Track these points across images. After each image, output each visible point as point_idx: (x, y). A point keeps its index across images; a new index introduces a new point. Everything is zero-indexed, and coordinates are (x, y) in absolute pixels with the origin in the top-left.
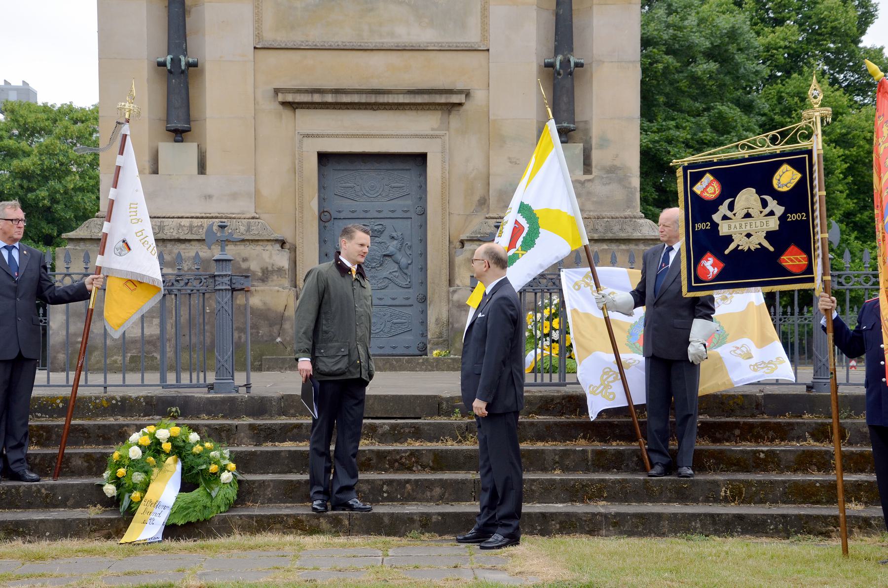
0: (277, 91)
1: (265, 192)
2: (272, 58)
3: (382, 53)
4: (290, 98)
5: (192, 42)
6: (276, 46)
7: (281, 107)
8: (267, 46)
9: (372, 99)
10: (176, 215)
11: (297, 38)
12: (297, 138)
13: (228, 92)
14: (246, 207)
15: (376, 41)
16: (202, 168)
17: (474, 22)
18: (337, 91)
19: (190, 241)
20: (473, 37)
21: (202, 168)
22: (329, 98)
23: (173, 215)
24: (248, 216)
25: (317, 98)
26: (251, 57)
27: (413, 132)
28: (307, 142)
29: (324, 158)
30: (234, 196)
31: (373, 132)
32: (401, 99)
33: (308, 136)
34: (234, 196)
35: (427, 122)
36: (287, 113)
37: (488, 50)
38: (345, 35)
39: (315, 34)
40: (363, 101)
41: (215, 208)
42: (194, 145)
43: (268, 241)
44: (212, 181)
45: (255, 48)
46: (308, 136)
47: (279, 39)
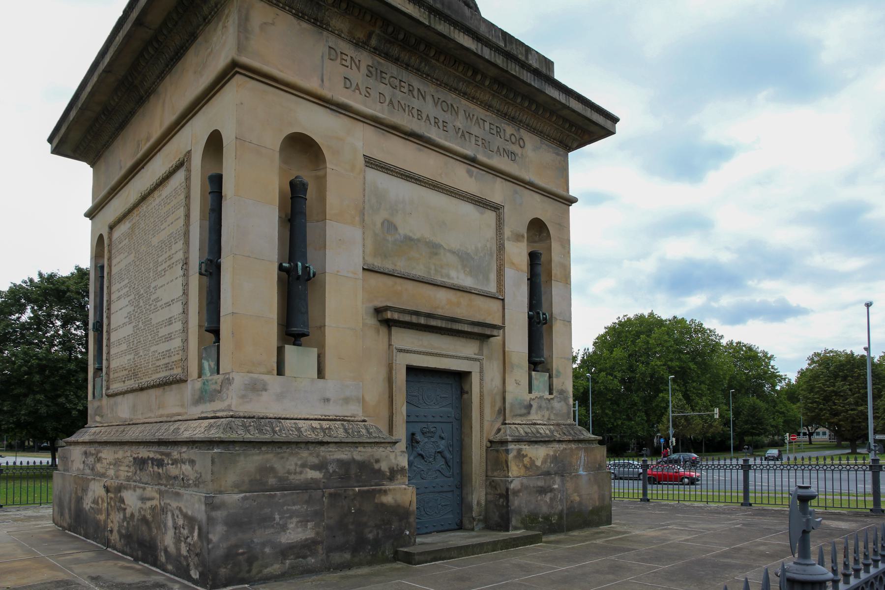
0: (378, 311)
1: (367, 398)
2: (375, 281)
3: (444, 289)
4: (396, 316)
5: (311, 253)
6: (376, 269)
7: (378, 323)
8: (371, 268)
9: (449, 325)
10: (303, 417)
11: (388, 266)
12: (395, 351)
13: (344, 302)
14: (354, 410)
15: (439, 279)
16: (321, 374)
17: (493, 276)
18: (429, 316)
19: (328, 443)
21: (321, 374)
22: (422, 321)
23: (299, 417)
24: (360, 419)
25: (414, 319)
26: (361, 276)
27: (465, 355)
28: (401, 355)
29: (412, 370)
30: (347, 400)
31: (444, 352)
32: (466, 328)
33: (400, 351)
34: (347, 400)
35: (469, 348)
36: (384, 330)
38: (419, 271)
39: (400, 265)
40: (444, 326)
41: (333, 410)
42: (315, 351)
43: (389, 443)
44: (330, 386)
45: (364, 269)
46: (400, 351)
47: (376, 264)
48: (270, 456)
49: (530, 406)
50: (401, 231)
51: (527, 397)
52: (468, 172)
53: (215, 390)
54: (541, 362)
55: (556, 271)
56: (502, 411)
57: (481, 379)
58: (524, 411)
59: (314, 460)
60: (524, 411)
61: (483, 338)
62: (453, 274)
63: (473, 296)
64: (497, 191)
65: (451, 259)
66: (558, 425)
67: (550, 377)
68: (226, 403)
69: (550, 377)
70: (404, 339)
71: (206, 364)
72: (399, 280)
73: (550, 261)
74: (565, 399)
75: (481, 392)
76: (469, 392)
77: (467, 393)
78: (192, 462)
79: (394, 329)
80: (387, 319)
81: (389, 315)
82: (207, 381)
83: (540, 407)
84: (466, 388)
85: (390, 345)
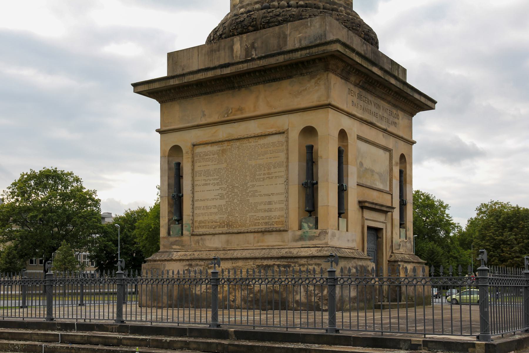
20: (388, 189)
29: (369, 228)
33: (367, 219)
37: (392, 195)
46: (367, 219)
48: (346, 262)
49: (400, 245)
50: (365, 166)
51: (399, 240)
52: (383, 135)
53: (314, 236)
54: (403, 224)
55: (408, 179)
56: (392, 247)
57: (386, 232)
58: (398, 247)
59: (355, 265)
60: (398, 247)
61: (386, 212)
62: (377, 183)
63: (384, 194)
64: (390, 143)
65: (376, 177)
66: (409, 254)
67: (406, 231)
68: (323, 242)
69: (406, 231)
70: (368, 214)
71: (305, 225)
72: (364, 188)
73: (406, 174)
74: (410, 242)
75: (386, 238)
76: (382, 238)
77: (380, 238)
78: (319, 265)
79: (364, 210)
80: (363, 206)
81: (367, 205)
82: (307, 232)
83: (403, 245)
84: (380, 235)
85: (363, 217)
